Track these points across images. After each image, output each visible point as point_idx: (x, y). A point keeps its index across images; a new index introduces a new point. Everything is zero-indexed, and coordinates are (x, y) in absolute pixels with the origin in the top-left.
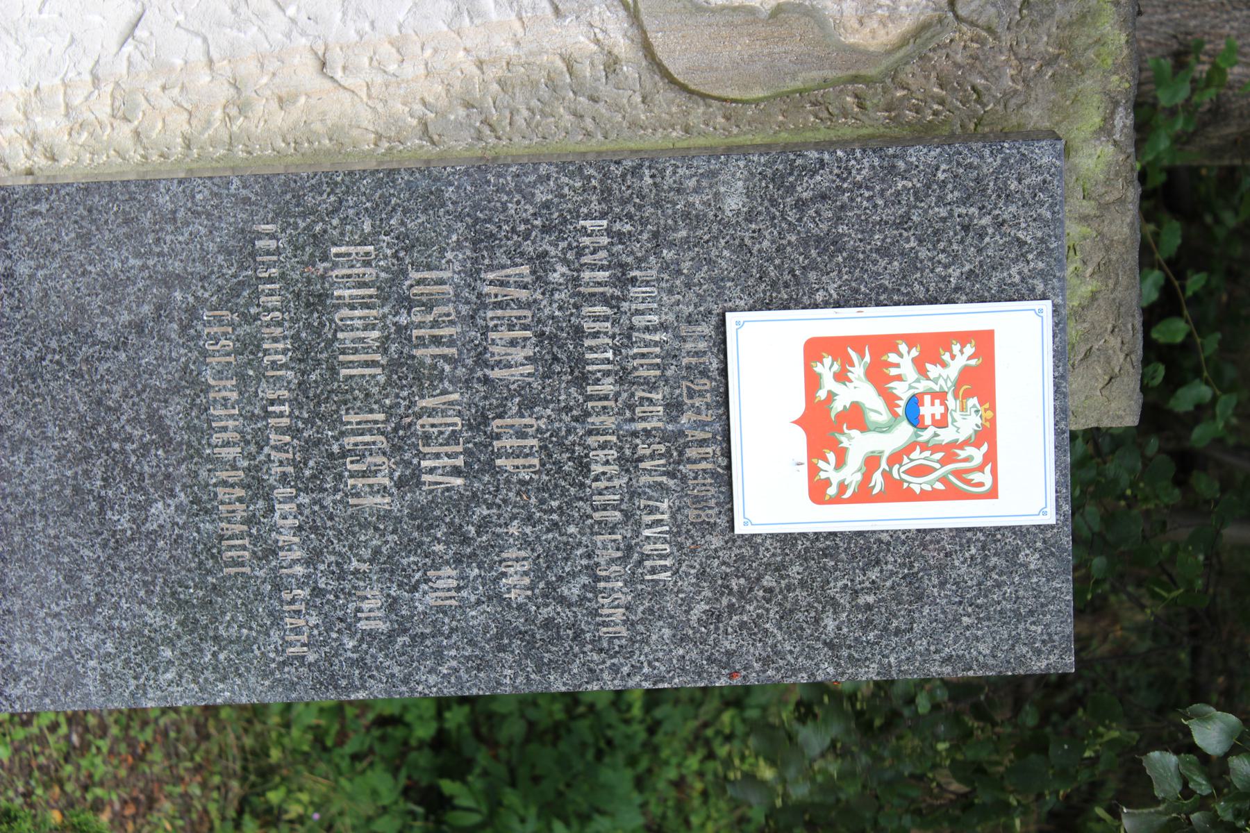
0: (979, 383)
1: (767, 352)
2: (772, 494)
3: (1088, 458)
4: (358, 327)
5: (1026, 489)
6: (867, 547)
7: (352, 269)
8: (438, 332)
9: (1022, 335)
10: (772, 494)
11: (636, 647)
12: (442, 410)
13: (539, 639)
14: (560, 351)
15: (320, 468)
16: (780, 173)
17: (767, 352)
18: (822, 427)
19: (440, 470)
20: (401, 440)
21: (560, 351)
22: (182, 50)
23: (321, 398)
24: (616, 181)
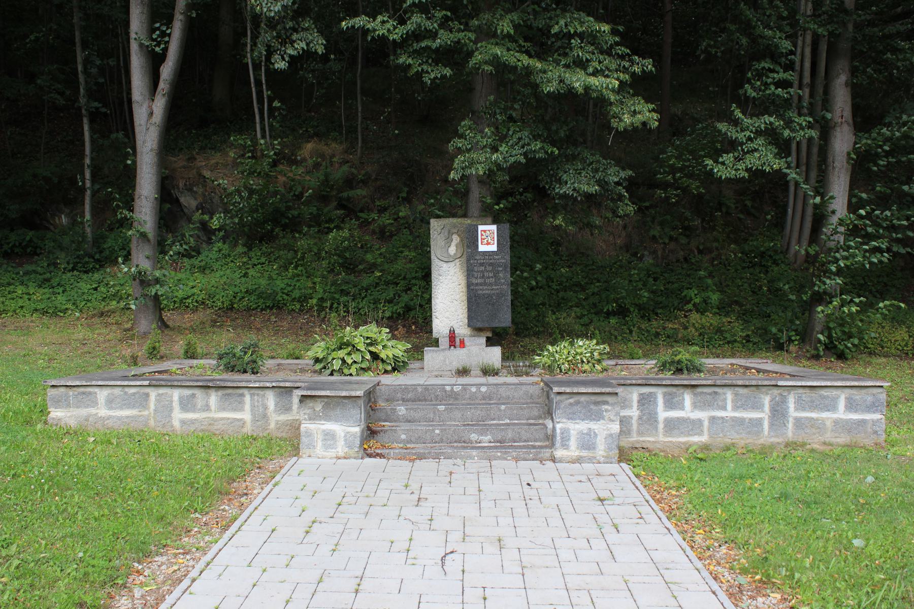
0: (485, 231)
1: (482, 248)
2: (494, 248)
3: (494, 223)
4: (479, 281)
5: (494, 228)
6: (498, 240)
7: (474, 281)
8: (480, 275)
9: (481, 228)
10: (494, 248)
11: (506, 259)
12: (486, 274)
13: (505, 267)
14: (482, 264)
15: (491, 284)
16: (468, 247)
17: (482, 248)
18: (488, 244)
19: (491, 275)
20: (489, 278)
21: (482, 264)
22: (458, 296)
23: (485, 284)
24: (468, 260)
